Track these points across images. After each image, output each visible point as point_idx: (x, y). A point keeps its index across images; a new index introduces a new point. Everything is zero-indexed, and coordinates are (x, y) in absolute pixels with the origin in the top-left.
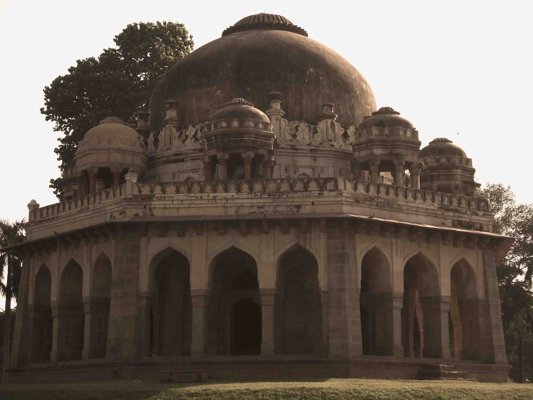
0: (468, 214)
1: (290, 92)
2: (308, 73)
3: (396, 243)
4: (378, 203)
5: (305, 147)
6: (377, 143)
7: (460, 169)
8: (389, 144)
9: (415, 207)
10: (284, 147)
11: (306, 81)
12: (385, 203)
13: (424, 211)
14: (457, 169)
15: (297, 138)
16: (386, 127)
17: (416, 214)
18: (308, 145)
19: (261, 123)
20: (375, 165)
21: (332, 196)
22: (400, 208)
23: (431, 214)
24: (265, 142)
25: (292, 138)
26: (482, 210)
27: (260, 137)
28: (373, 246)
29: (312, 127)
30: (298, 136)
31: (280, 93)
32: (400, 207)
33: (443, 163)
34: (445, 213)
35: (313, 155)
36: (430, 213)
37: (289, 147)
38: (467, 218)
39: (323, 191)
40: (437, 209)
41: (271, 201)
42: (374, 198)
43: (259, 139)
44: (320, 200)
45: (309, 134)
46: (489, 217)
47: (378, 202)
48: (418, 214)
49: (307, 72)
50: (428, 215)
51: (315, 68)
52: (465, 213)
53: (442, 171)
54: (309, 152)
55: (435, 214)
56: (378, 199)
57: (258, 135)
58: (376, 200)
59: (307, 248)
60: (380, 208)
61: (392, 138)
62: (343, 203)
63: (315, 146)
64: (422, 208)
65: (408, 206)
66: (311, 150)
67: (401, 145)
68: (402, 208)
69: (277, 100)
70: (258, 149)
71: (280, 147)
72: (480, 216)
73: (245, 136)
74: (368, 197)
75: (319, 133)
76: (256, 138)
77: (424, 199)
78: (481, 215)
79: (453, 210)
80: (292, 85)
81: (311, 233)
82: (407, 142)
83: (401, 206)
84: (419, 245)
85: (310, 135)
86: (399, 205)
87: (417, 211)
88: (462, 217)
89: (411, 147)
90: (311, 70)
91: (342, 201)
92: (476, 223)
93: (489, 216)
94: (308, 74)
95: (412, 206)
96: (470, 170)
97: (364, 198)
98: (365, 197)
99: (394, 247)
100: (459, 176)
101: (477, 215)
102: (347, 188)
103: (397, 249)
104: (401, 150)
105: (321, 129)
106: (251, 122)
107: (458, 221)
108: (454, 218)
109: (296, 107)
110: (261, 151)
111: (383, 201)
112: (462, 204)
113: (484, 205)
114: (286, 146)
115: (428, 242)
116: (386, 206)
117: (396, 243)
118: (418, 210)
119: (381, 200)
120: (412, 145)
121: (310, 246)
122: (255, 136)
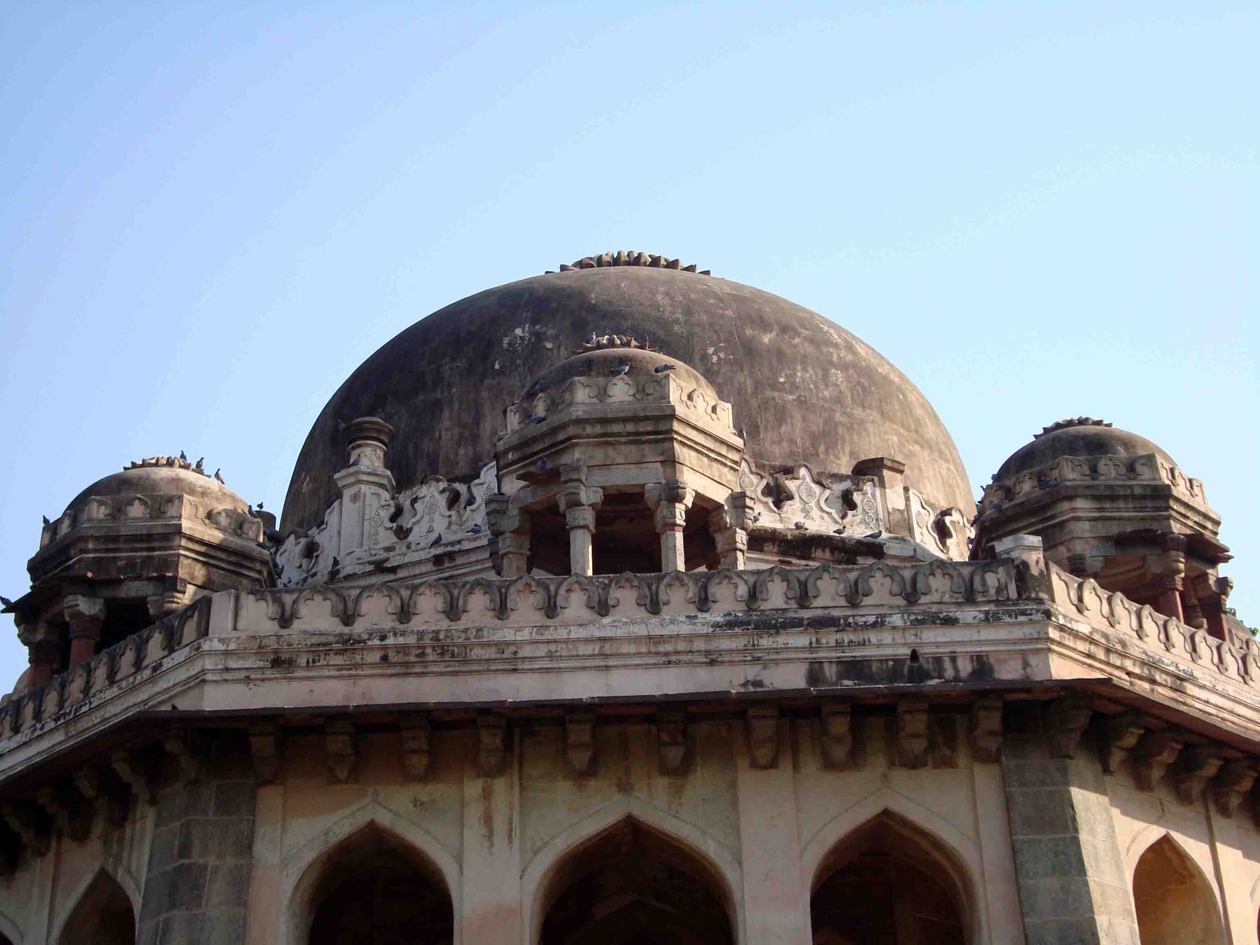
0: (894, 628)
1: (446, 413)
2: (506, 341)
3: (487, 795)
4: (393, 657)
5: (413, 557)
6: (510, 456)
7: (1086, 497)
8: (540, 446)
9: (587, 641)
10: (355, 574)
11: (497, 367)
12: (424, 648)
13: (644, 650)
14: (1070, 498)
15: (411, 538)
16: (540, 395)
17: (598, 668)
18: (431, 545)
19: (137, 502)
20: (502, 533)
21: (180, 665)
22: (505, 656)
23: (683, 658)
24: (148, 557)
25: (395, 540)
26: (997, 602)
27: (122, 546)
28: (362, 820)
29: (461, 488)
30: (416, 529)
31: (380, 421)
32: (508, 653)
33: (1027, 494)
34: (765, 642)
35: (446, 575)
36: (677, 653)
37: (370, 568)
38: (894, 645)
39: (172, 651)
40: (711, 630)
41: (62, 738)
42: (365, 636)
43: (127, 551)
44: (162, 685)
45: (449, 513)
46: (1021, 624)
47: (385, 648)
48: (607, 667)
49: (502, 341)
50: (664, 659)
51: (534, 322)
52: (879, 624)
53: (1021, 525)
54: (434, 569)
55: (707, 653)
56: (383, 638)
57: (111, 539)
58: (377, 642)
59: (119, 879)
60: (402, 670)
61: (555, 419)
62: (204, 681)
63: (446, 545)
64: (636, 640)
65: (549, 642)
66: (438, 560)
67: (578, 437)
68: (518, 656)
69: (358, 442)
70: (118, 582)
71: (341, 575)
72: (968, 625)
73: (73, 552)
74: (331, 639)
75: (479, 501)
76: (107, 550)
77: (655, 607)
78: (970, 620)
79: (806, 622)
80: (454, 390)
81: (134, 822)
82: (604, 421)
83: (513, 648)
84: (624, 787)
85: (450, 516)
86: (501, 646)
87: (606, 656)
88: (863, 644)
89: (629, 434)
90: (518, 332)
91: (203, 671)
92: (953, 660)
93: (1022, 618)
94: (505, 345)
95: (567, 641)
96: (1138, 491)
97: (312, 645)
98: (315, 640)
99: (474, 813)
100: (1087, 525)
101: (950, 622)
102: (240, 625)
103: (488, 820)
104: (577, 454)
105: (486, 485)
106: (95, 505)
107: (840, 662)
108: (822, 654)
109: (462, 452)
110: (132, 589)
111: (412, 640)
112: (867, 594)
113: (1003, 581)
114: (359, 569)
115: (680, 772)
116: (430, 658)
117: (487, 795)
118: (608, 648)
119: (401, 640)
120: (630, 427)
121: (129, 872)
122: (102, 546)
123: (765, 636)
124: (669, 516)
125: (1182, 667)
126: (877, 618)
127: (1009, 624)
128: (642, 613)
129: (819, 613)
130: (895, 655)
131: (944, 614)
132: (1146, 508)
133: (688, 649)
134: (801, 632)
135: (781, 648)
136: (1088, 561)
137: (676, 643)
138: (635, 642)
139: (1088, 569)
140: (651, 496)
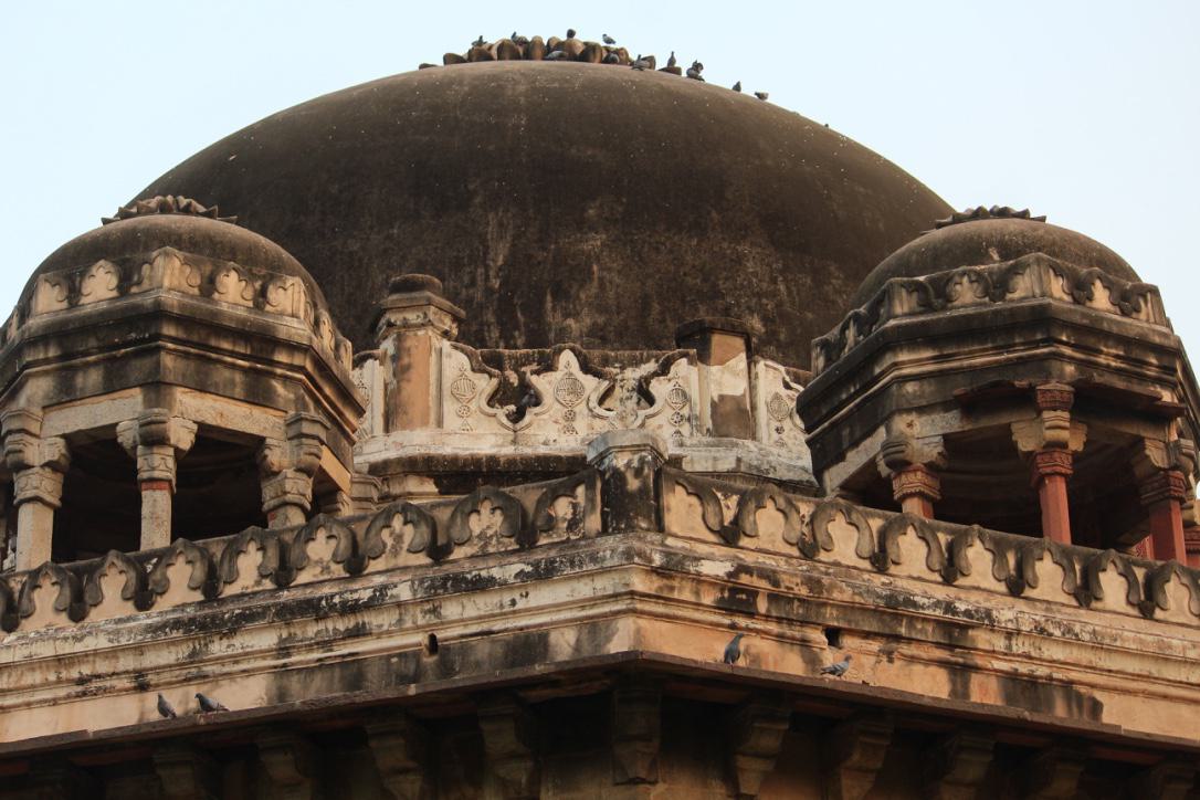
34: (218, 648)
88: (358, 632)
123: (216, 638)
124: (146, 468)
125: (962, 607)
126: (374, 592)
127: (569, 578)
128: (63, 620)
129: (299, 594)
130: (400, 647)
131: (474, 573)
132: (1015, 345)
133: (111, 670)
134: (263, 628)
135: (240, 655)
136: (916, 444)
137: (94, 662)
138: (41, 667)
139: (914, 460)
140: (127, 435)
